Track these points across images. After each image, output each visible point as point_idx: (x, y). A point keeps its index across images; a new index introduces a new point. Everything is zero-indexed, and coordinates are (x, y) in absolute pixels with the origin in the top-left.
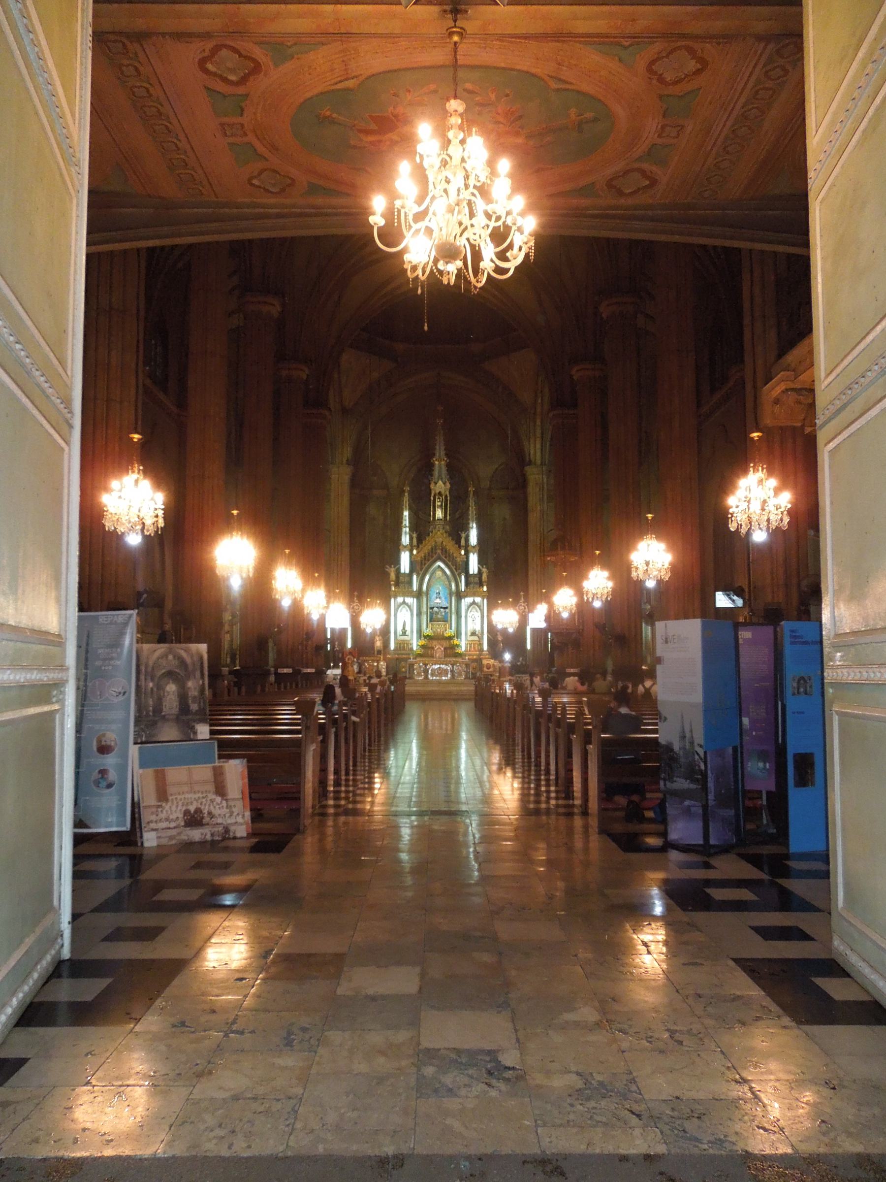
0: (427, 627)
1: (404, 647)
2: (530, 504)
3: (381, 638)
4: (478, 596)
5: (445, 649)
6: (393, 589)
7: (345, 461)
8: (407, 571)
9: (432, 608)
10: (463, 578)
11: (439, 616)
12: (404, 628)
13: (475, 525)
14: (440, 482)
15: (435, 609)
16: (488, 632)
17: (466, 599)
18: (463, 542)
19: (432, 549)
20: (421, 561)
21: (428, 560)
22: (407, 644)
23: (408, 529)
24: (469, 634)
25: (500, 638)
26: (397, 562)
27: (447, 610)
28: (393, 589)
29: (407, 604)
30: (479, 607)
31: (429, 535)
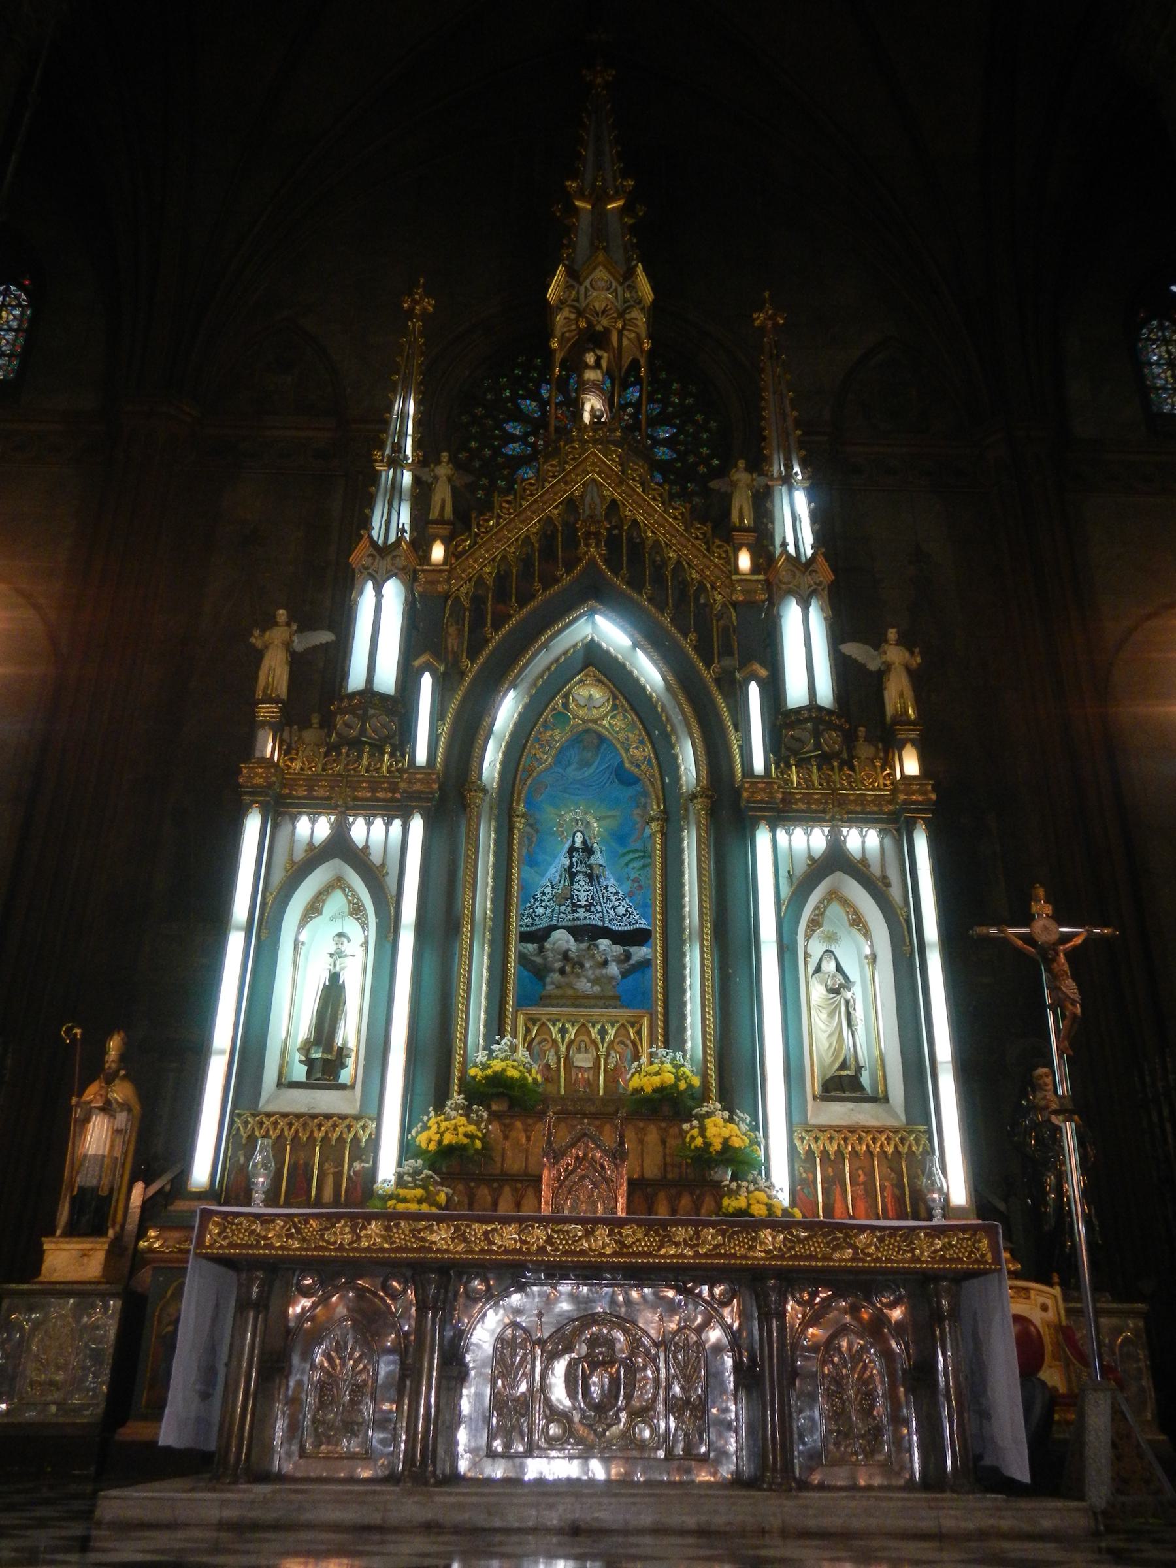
0: (497, 1025)
1: (300, 1174)
3: (121, 1092)
4: (861, 817)
5: (631, 1182)
6: (269, 747)
9: (538, 936)
10: (754, 690)
11: (584, 986)
13: (797, 469)
14: (601, 256)
15: (562, 939)
17: (781, 834)
18: (742, 510)
20: (477, 601)
21: (522, 604)
22: (333, 1151)
23: (407, 477)
24: (813, 1084)
27: (640, 952)
28: (269, 747)
29: (358, 858)
30: (877, 888)
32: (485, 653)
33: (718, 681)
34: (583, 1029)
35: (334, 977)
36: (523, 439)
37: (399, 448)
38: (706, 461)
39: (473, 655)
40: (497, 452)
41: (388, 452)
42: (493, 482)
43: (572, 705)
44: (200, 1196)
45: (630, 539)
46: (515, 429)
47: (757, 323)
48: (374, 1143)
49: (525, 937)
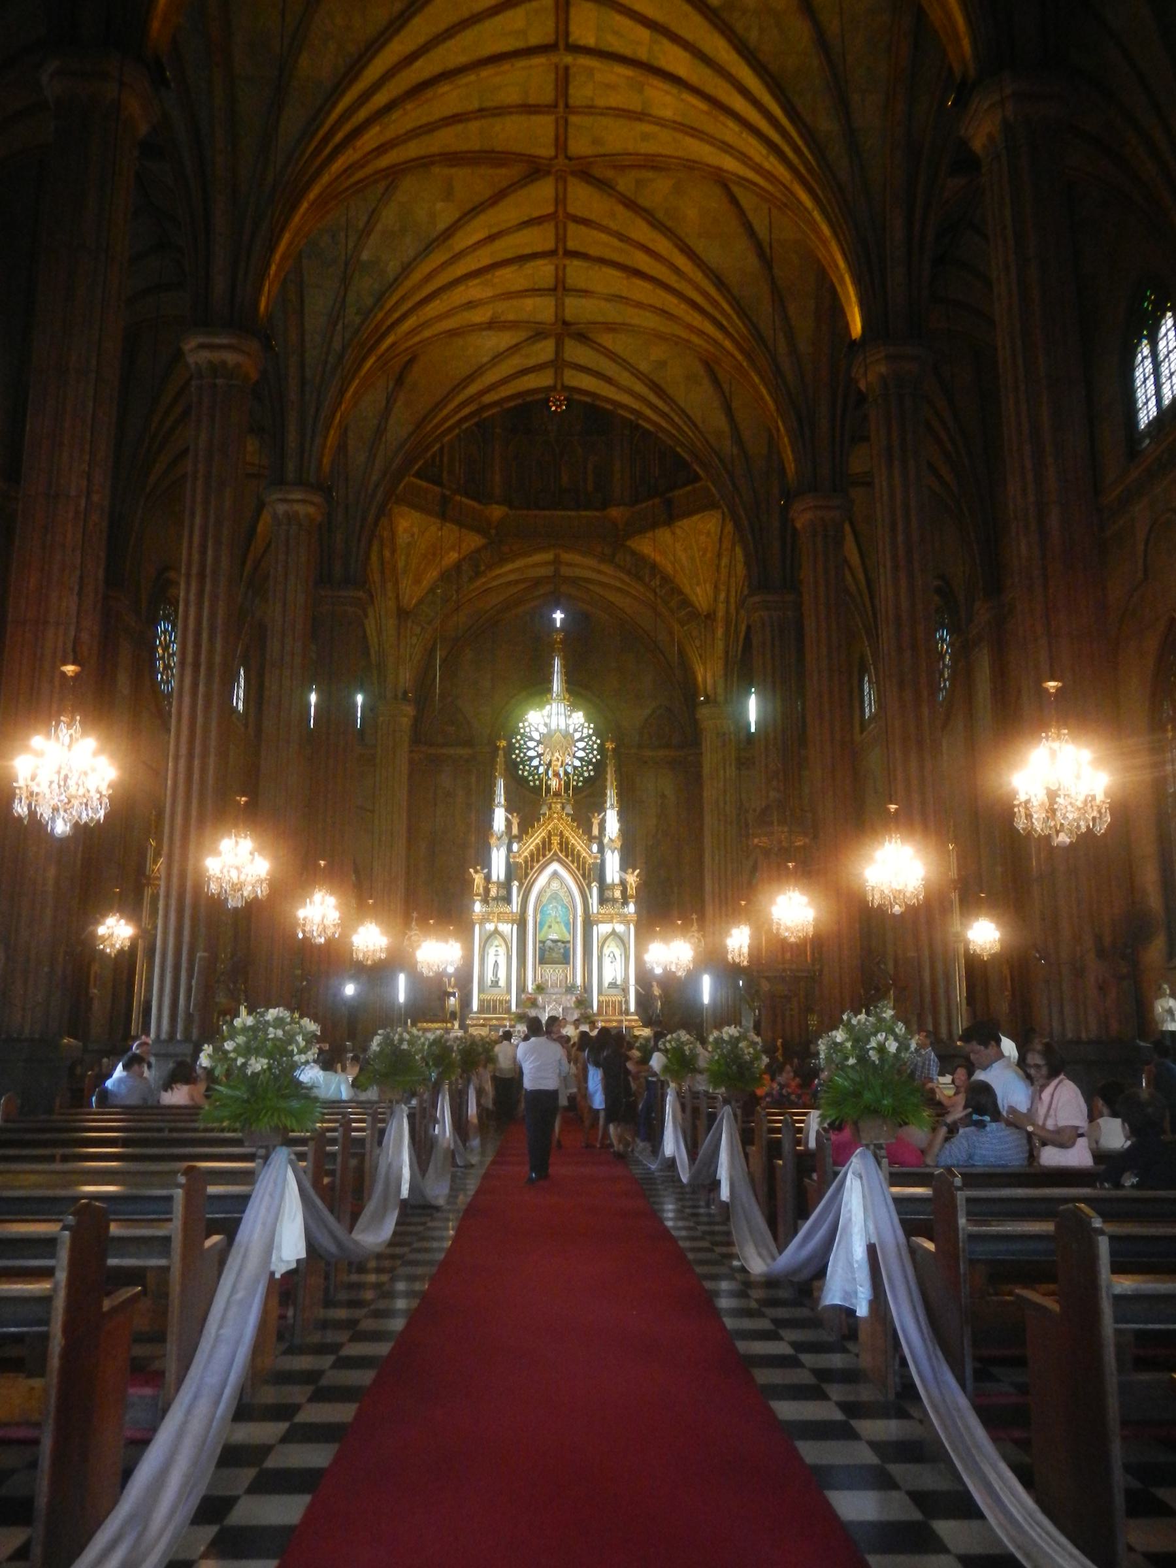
1: (495, 1007)
2: (706, 770)
7: (400, 695)
8: (502, 877)
10: (595, 891)
11: (554, 955)
12: (495, 974)
16: (638, 981)
17: (600, 925)
18: (595, 832)
19: (544, 842)
20: (526, 862)
21: (538, 861)
24: (606, 984)
25: (657, 991)
26: (486, 863)
27: (568, 945)
31: (539, 820)
32: (529, 878)
34: (554, 971)
35: (496, 962)
36: (534, 749)
38: (595, 757)
40: (525, 754)
42: (524, 767)
44: (476, 1013)
46: (531, 744)
48: (509, 1002)
49: (540, 942)
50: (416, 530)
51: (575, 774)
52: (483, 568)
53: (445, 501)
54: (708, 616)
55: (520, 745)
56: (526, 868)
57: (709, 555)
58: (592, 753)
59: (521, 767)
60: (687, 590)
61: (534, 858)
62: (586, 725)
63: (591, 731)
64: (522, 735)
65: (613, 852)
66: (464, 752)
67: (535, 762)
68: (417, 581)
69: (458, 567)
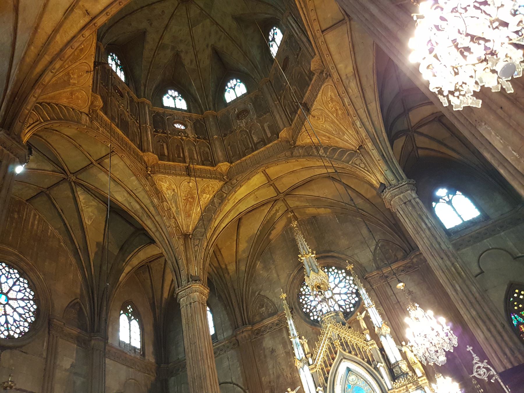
19: (329, 348)
20: (322, 369)
21: (331, 366)
33: (374, 368)
37: (293, 334)
38: (354, 288)
39: (327, 383)
40: (311, 306)
41: (292, 335)
42: (313, 314)
43: (350, 382)
45: (344, 342)
47: (348, 269)
50: (174, 187)
51: (346, 304)
52: (225, 196)
53: (188, 168)
54: (361, 147)
55: (306, 301)
56: (324, 374)
57: (340, 112)
58: (351, 287)
59: (311, 314)
60: (341, 144)
61: (327, 364)
62: (340, 272)
63: (344, 275)
64: (305, 295)
65: (385, 336)
66: (275, 319)
67: (319, 308)
68: (189, 216)
69: (212, 202)
